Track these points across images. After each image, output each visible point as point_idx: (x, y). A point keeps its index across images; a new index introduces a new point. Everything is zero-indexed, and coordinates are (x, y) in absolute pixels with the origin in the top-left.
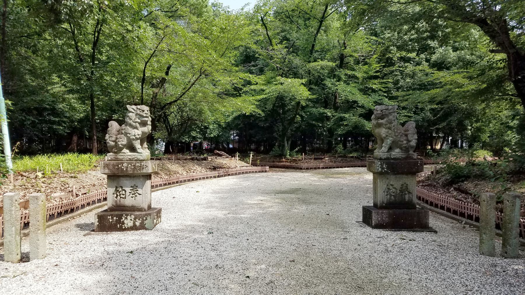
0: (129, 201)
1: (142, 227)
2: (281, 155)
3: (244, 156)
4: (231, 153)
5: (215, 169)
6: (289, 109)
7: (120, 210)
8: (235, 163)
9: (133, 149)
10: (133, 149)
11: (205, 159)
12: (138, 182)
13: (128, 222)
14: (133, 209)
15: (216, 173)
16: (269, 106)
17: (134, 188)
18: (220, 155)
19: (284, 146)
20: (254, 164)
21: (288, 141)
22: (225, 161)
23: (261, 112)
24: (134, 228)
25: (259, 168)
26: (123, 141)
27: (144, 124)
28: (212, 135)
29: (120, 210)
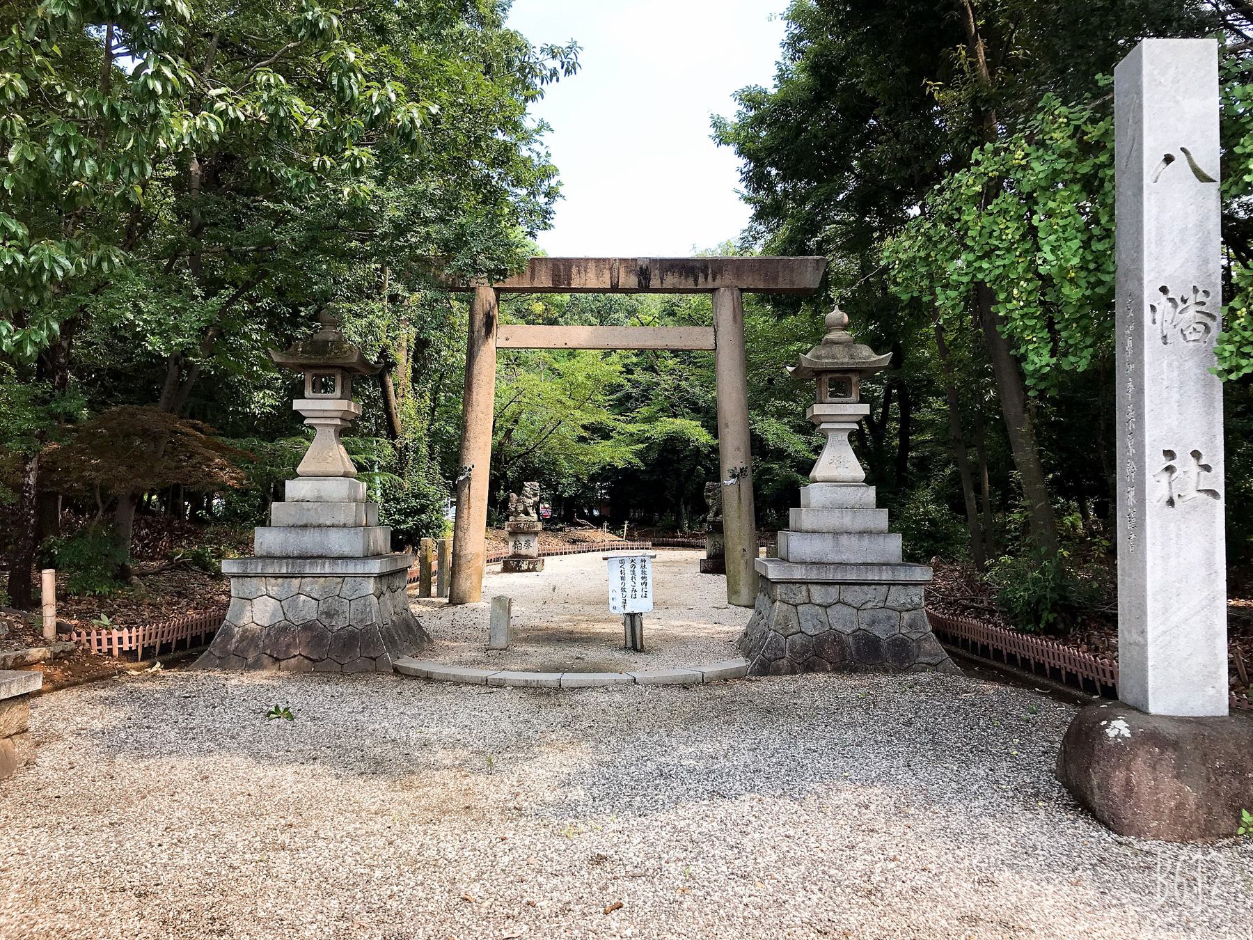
0: (523, 552)
1: (534, 570)
2: (677, 526)
3: (615, 528)
4: (597, 523)
5: (574, 542)
6: (685, 457)
7: (517, 557)
8: (602, 535)
9: (527, 514)
10: (527, 514)
11: (561, 529)
12: (530, 537)
13: (525, 566)
14: (526, 557)
15: (576, 548)
16: (654, 455)
17: (528, 542)
18: (582, 525)
19: (679, 514)
20: (630, 537)
21: (686, 504)
22: (589, 533)
23: (640, 464)
24: (528, 570)
25: (638, 544)
26: (521, 508)
27: (535, 495)
28: (566, 495)
29: (517, 557)
